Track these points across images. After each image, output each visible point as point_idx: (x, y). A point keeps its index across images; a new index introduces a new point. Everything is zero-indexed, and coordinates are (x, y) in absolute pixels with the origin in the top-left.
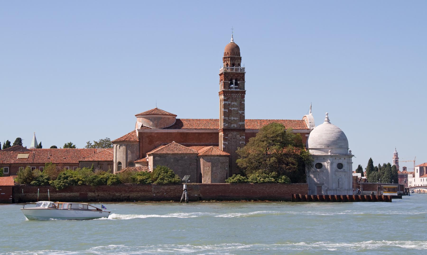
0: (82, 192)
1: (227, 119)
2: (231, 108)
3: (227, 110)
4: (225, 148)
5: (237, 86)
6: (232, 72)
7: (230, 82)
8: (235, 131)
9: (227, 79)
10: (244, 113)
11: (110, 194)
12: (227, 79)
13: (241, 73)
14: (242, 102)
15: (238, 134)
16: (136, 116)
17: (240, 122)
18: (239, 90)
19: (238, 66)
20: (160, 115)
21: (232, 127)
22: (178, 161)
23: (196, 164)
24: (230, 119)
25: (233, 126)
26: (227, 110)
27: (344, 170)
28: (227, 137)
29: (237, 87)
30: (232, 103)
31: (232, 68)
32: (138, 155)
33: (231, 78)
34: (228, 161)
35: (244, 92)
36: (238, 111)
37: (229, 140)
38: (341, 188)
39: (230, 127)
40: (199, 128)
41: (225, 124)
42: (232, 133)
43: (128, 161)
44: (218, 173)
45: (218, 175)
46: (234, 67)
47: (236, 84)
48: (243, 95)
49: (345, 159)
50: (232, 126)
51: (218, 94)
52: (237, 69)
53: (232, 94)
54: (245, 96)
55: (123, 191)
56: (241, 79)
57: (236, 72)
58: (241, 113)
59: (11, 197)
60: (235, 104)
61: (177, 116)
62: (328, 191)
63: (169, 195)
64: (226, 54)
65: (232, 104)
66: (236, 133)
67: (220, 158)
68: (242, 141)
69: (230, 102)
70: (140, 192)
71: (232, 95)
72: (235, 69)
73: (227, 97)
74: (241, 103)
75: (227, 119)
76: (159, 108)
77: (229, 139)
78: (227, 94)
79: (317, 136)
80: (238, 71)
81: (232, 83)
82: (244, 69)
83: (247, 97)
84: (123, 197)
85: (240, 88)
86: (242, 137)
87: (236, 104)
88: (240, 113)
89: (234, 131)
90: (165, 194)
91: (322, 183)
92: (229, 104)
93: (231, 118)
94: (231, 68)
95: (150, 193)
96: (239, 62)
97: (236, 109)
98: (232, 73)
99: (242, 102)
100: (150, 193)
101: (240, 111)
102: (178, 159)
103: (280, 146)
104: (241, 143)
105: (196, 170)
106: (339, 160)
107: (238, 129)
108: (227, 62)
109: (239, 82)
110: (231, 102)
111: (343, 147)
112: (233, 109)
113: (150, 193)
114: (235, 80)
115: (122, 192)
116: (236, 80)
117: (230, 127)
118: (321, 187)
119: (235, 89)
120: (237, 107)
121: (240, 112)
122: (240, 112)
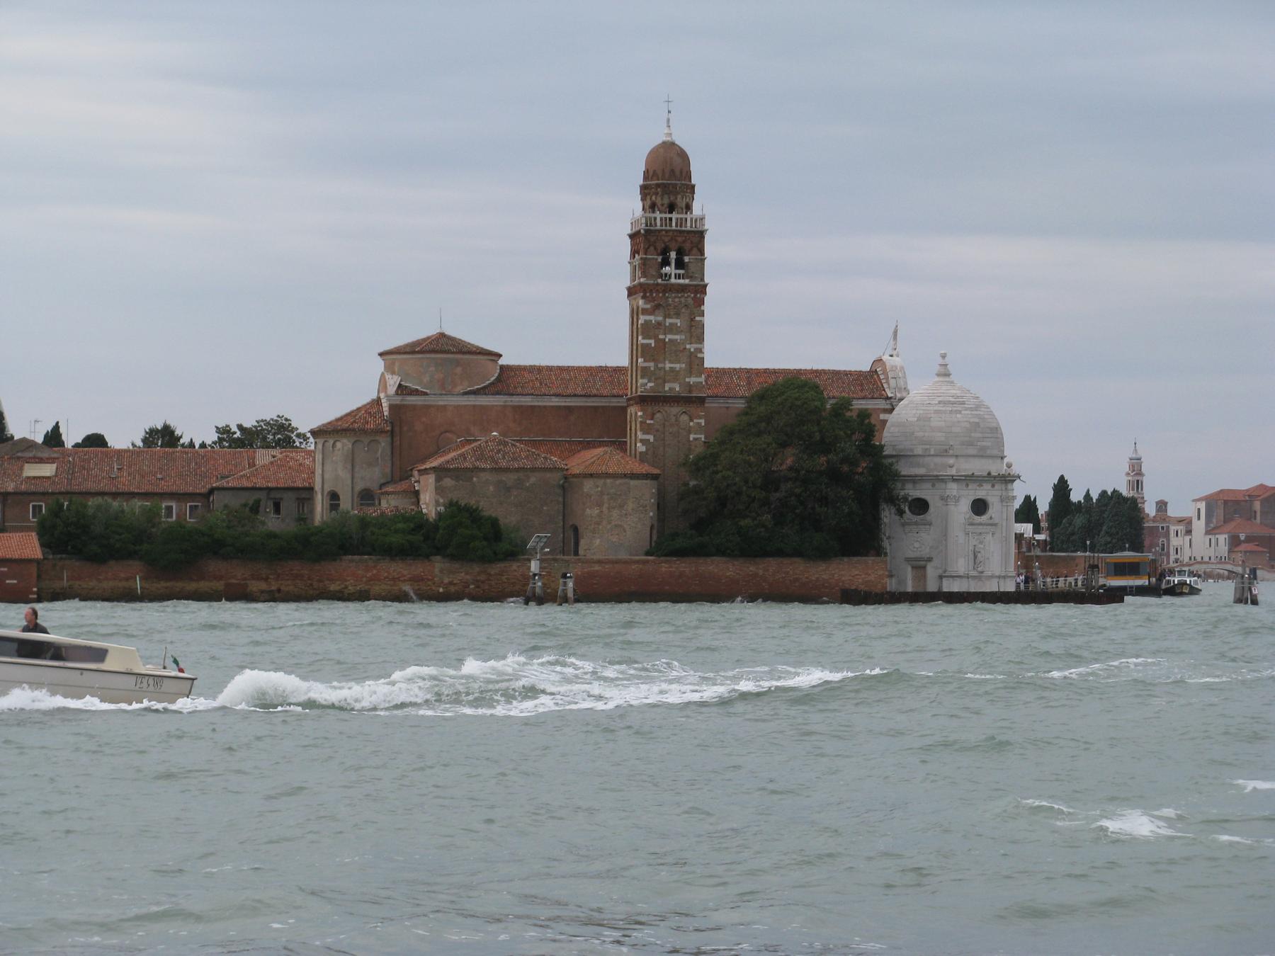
0: (233, 581)
1: (652, 369)
2: (665, 334)
3: (652, 342)
4: (647, 454)
5: (682, 272)
6: (668, 228)
7: (661, 257)
8: (676, 404)
9: (652, 248)
10: (701, 351)
11: (311, 585)
12: (652, 248)
13: (693, 231)
14: (698, 318)
15: (684, 412)
16: (381, 355)
18: (687, 281)
21: (665, 392)
22: (508, 489)
23: (561, 499)
24: (660, 369)
26: (652, 342)
27: (991, 518)
28: (652, 422)
30: (668, 321)
31: (668, 216)
32: (388, 470)
33: (663, 245)
34: (654, 491)
35: (702, 289)
36: (683, 343)
37: (657, 431)
38: (982, 572)
39: (660, 392)
40: (569, 392)
42: (666, 408)
43: (358, 488)
44: (625, 526)
45: (625, 532)
46: (674, 216)
47: (680, 264)
49: (993, 486)
50: (667, 389)
51: (626, 293)
52: (681, 219)
55: (349, 578)
56: (695, 250)
57: (679, 228)
58: (692, 350)
59: (33, 593)
61: (501, 356)
62: (944, 579)
63: (483, 590)
64: (651, 174)
65: (667, 324)
66: (680, 408)
67: (633, 483)
68: (695, 434)
69: (660, 318)
70: (399, 581)
71: (668, 297)
73: (653, 304)
74: (692, 320)
75: (652, 369)
76: (450, 332)
77: (658, 427)
78: (651, 295)
79: (916, 419)
80: (686, 227)
81: (666, 262)
82: (702, 219)
84: (349, 594)
86: (695, 421)
88: (690, 349)
89: (672, 404)
90: (472, 587)
91: (928, 556)
92: (659, 324)
94: (666, 218)
95: (430, 583)
96: (688, 200)
97: (677, 340)
98: (667, 231)
99: (698, 318)
100: (429, 586)
101: (691, 344)
102: (508, 486)
104: (691, 439)
105: (561, 518)
106: (976, 489)
107: (683, 397)
108: (654, 198)
109: (686, 259)
110: (665, 318)
111: (989, 452)
112: (669, 339)
113: (429, 586)
115: (346, 581)
116: (680, 253)
117: (660, 390)
118: (924, 567)
119: (676, 278)
120: (679, 331)
121: (692, 347)
122: (692, 347)
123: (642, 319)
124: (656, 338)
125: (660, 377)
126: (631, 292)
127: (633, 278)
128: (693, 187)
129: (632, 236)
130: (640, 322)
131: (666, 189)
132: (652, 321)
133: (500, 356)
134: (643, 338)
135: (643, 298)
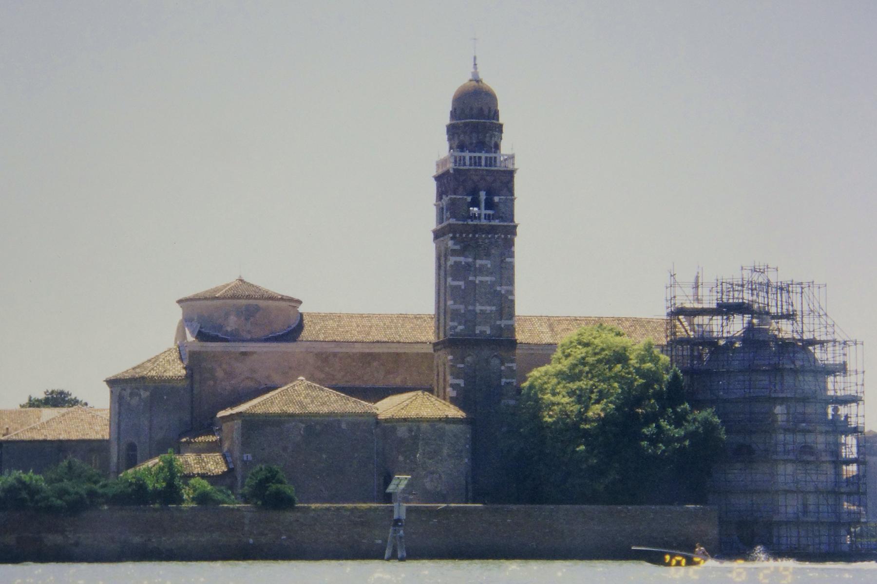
2: (475, 276)
3: (461, 283)
10: (511, 293)
12: (461, 189)
14: (508, 260)
16: (180, 302)
17: (501, 319)
18: (496, 222)
19: (493, 150)
20: (255, 299)
21: (476, 335)
25: (480, 331)
28: (462, 366)
29: (493, 215)
30: (479, 262)
31: (477, 155)
34: (468, 436)
35: (511, 231)
41: (456, 327)
47: (490, 205)
48: (509, 236)
51: (432, 236)
52: (491, 158)
53: (477, 236)
54: (517, 240)
57: (488, 168)
60: (487, 265)
69: (470, 260)
71: (477, 238)
72: (486, 158)
74: (502, 261)
78: (461, 235)
82: (512, 157)
83: (519, 242)
85: (502, 217)
87: (489, 266)
92: (468, 264)
93: (475, 306)
94: (475, 157)
97: (487, 281)
98: (476, 170)
99: (508, 260)
103: (628, 391)
109: (496, 199)
110: (475, 259)
114: (485, 193)
116: (490, 193)
122: (503, 289)
123: (452, 260)
124: (465, 279)
125: (470, 319)
126: (438, 235)
127: (440, 220)
128: (501, 126)
129: (438, 178)
130: (449, 263)
131: (475, 128)
132: (461, 262)
133: (299, 302)
134: (453, 280)
135: (452, 238)
